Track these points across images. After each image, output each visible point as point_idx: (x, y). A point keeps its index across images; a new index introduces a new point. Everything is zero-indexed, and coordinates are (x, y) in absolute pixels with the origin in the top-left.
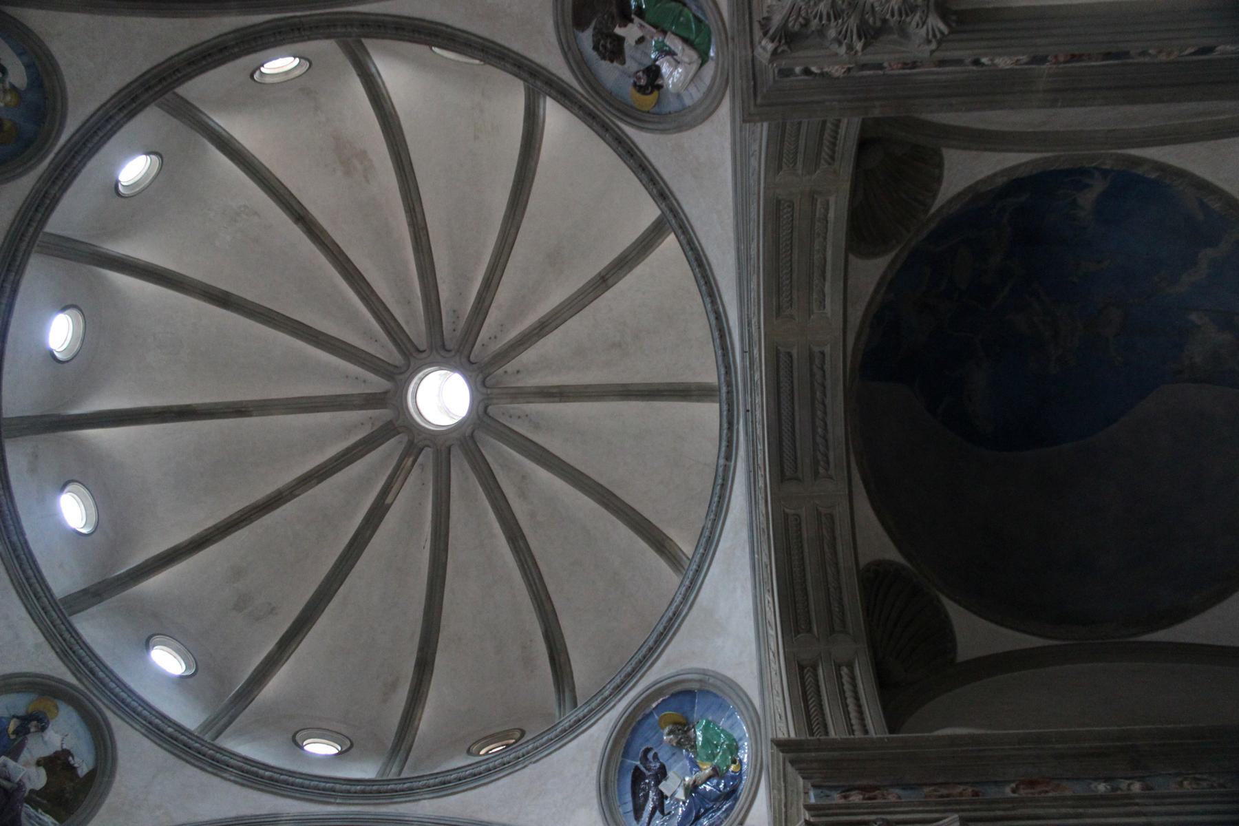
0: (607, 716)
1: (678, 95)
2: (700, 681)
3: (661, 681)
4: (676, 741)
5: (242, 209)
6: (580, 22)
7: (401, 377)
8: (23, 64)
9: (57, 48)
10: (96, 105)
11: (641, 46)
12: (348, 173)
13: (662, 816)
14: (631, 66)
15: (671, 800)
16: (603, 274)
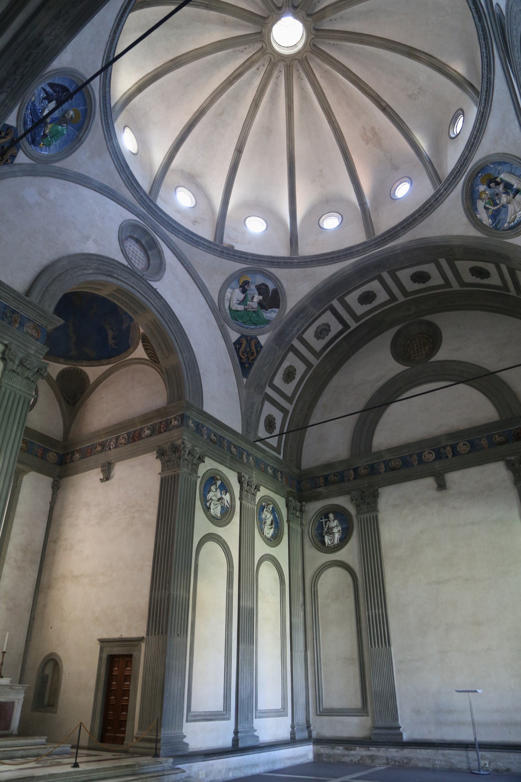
0: (98, 87)
1: (233, 289)
2: (81, 139)
3: (93, 120)
4: (67, 117)
5: (417, 97)
6: (276, 292)
7: (311, 38)
8: (478, 211)
9: (464, 219)
10: (451, 195)
11: (252, 296)
12: (373, 128)
13: (43, 97)
14: (253, 287)
15: (46, 104)
16: (241, 154)
